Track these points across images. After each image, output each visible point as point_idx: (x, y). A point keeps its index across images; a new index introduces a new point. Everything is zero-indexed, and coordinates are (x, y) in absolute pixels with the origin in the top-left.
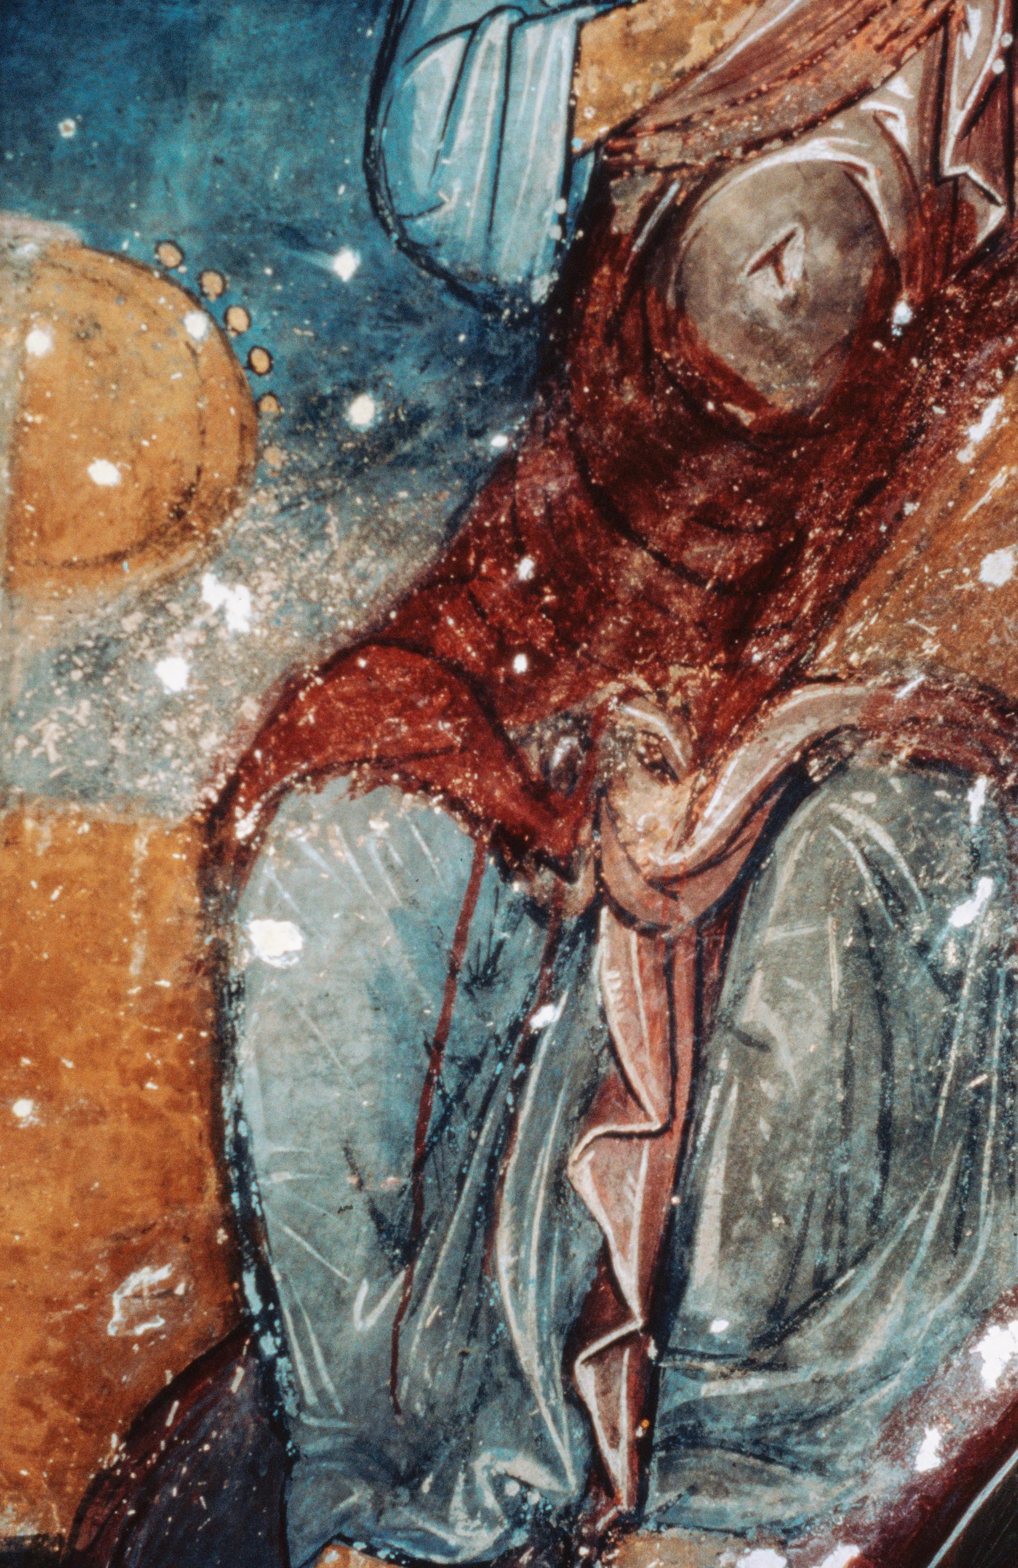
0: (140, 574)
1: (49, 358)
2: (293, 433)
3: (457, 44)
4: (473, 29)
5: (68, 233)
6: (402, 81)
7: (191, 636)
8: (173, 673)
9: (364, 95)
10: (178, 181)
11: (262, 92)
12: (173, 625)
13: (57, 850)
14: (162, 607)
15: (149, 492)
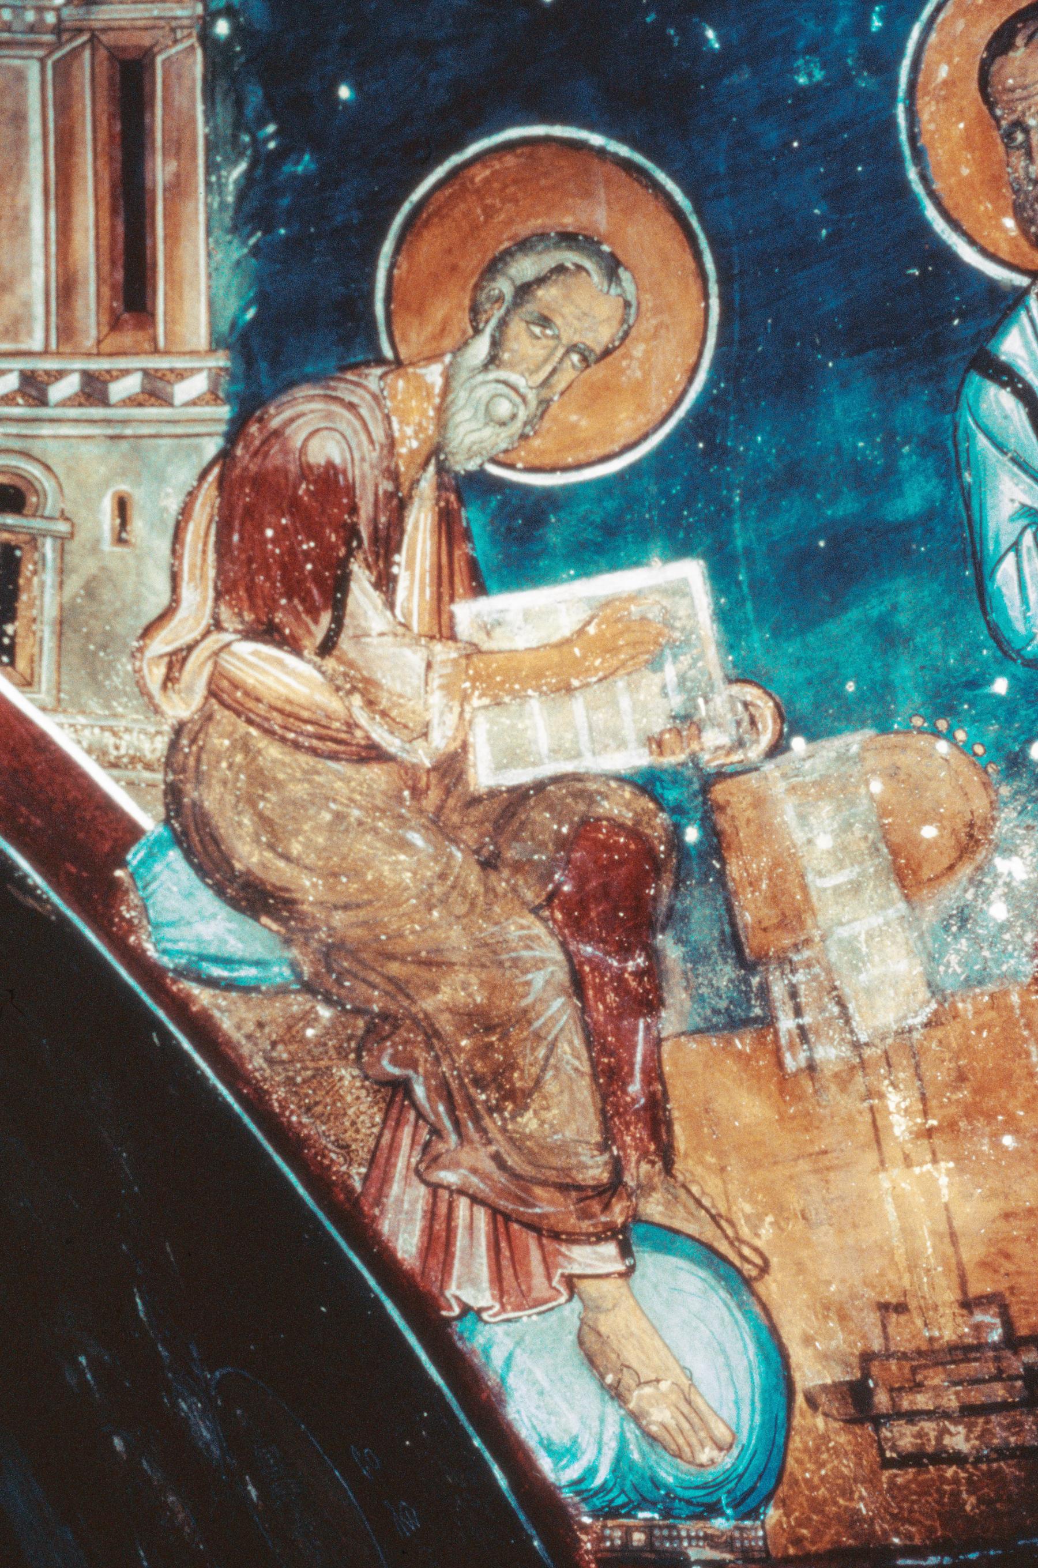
0: (966, 870)
1: (884, 792)
2: (1008, 776)
3: (1011, 557)
4: (1016, 546)
5: (869, 732)
6: (991, 588)
7: (1000, 890)
8: (999, 911)
9: (977, 604)
10: (909, 685)
11: (929, 626)
12: (990, 888)
13: (977, 1013)
14: (981, 882)
15: (953, 831)
